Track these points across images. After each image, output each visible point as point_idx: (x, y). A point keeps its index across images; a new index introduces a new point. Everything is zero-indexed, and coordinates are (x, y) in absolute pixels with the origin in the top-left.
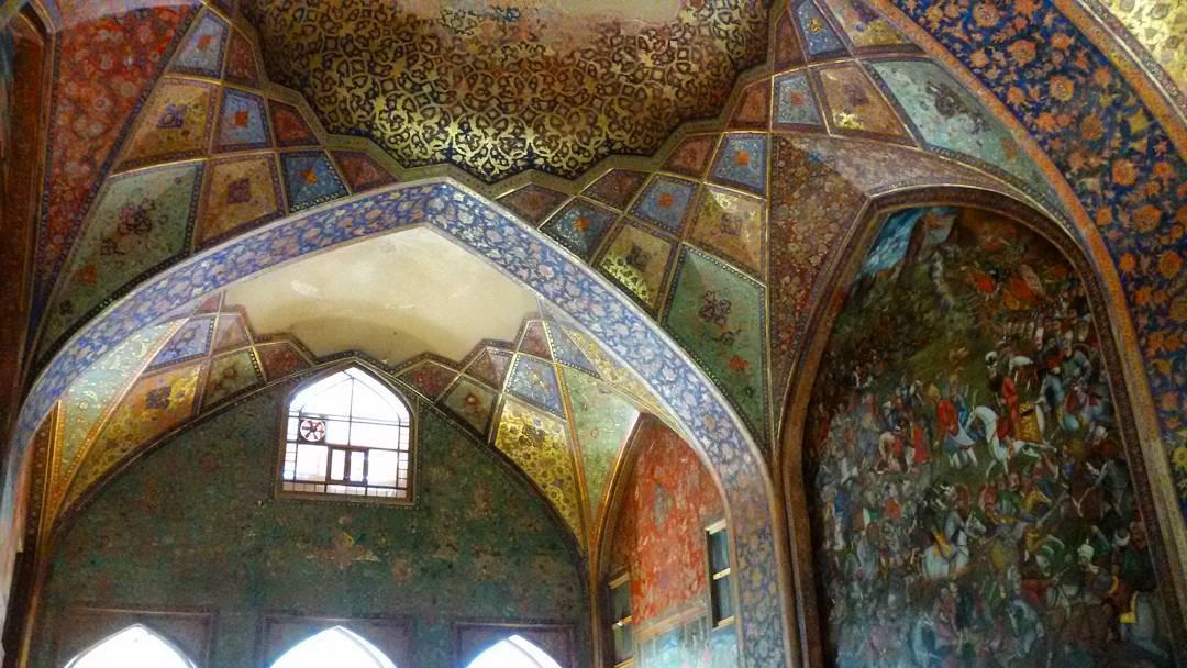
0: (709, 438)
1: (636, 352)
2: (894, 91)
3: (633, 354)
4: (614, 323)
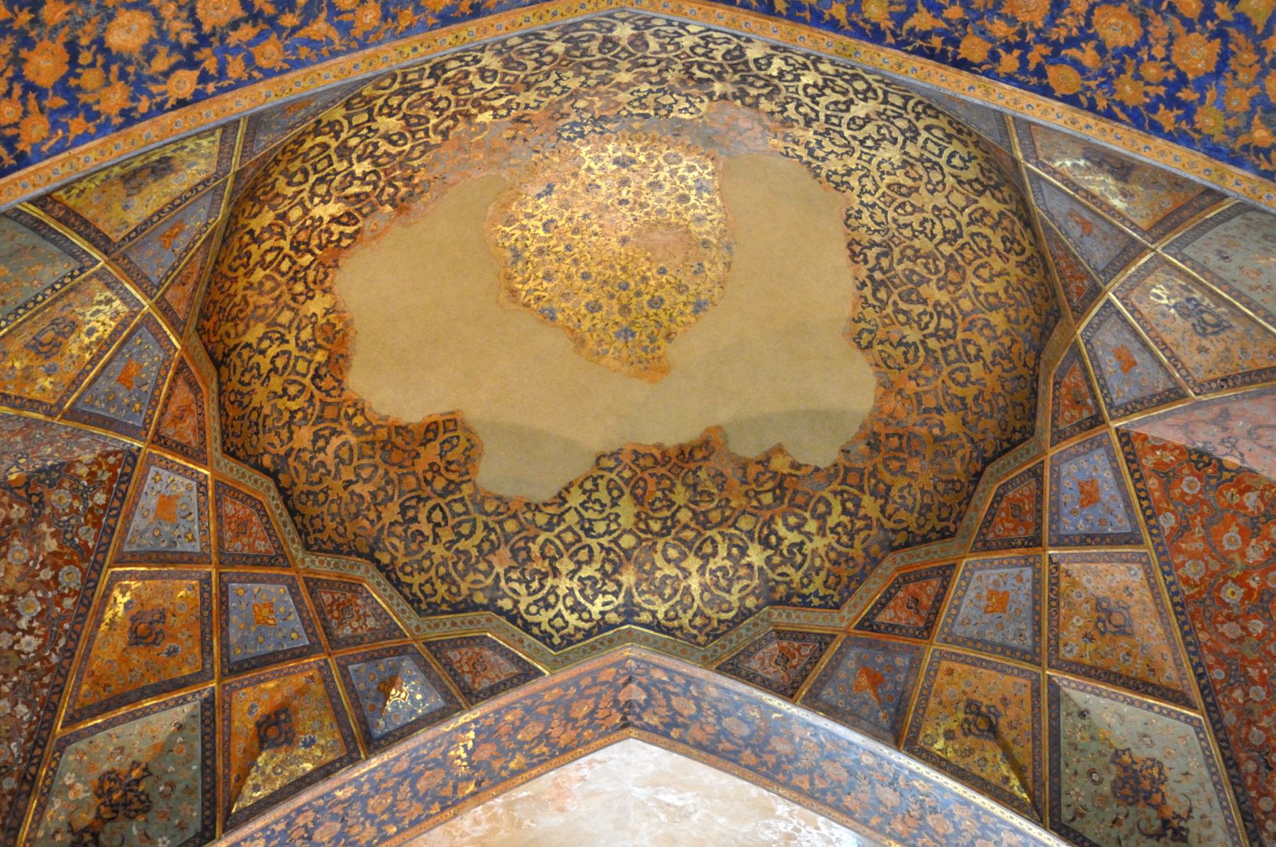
2: (153, 718)
4: (72, 48)
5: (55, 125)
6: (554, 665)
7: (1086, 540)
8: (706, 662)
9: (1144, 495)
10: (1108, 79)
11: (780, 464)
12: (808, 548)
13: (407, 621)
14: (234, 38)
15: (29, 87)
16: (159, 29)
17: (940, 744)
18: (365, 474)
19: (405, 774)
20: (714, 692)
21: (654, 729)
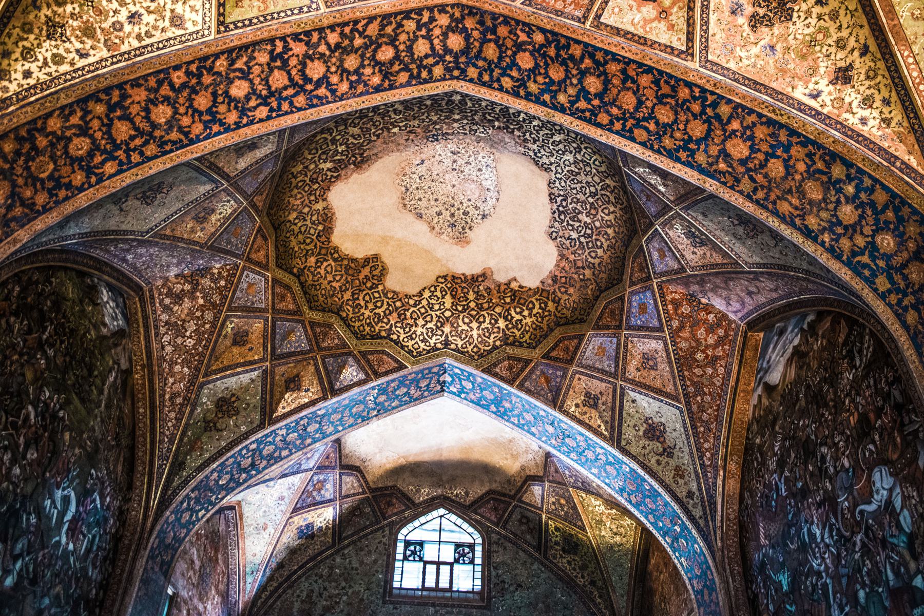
0: (18, 153)
1: (166, 99)
3: (165, 90)
4: (215, 95)
5: (205, 128)
6: (413, 364)
7: (640, 328)
8: (477, 367)
9: (666, 311)
10: (659, 138)
11: (514, 285)
12: (524, 322)
13: (351, 342)
14: (285, 94)
15: (196, 111)
16: (252, 88)
17: (573, 409)
18: (337, 278)
19: (346, 406)
20: (479, 380)
21: (454, 394)
